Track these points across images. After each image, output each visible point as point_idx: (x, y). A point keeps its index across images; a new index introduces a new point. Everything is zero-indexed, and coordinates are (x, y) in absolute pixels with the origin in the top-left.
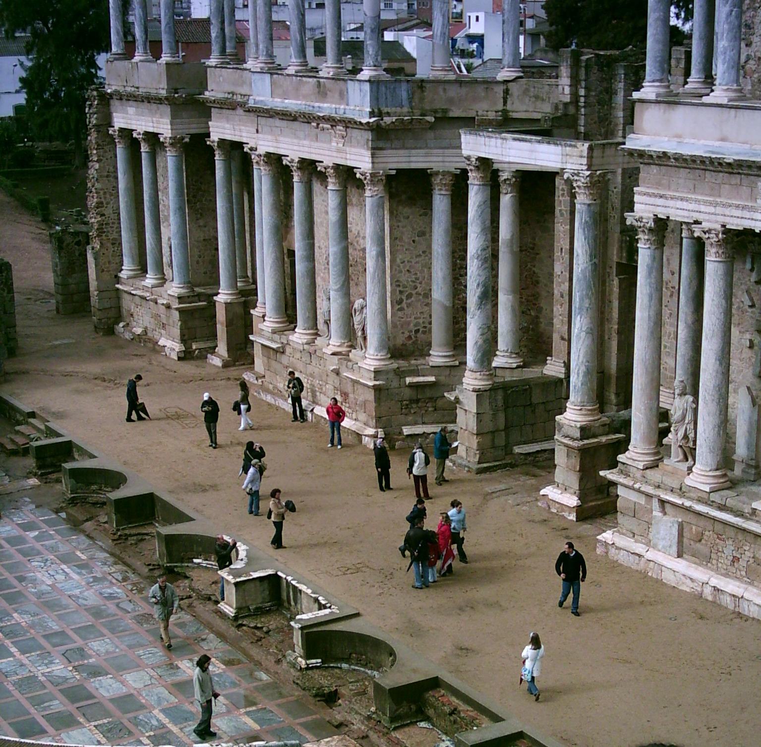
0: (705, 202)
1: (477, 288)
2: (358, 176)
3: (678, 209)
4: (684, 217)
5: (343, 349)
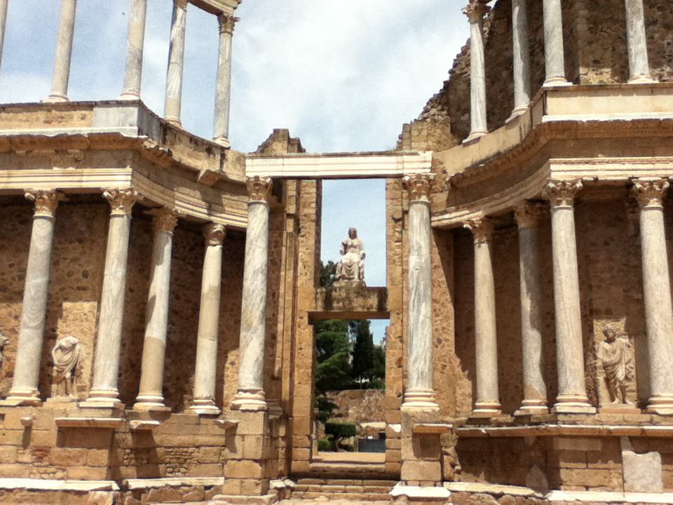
0: (642, 162)
1: (261, 302)
2: (106, 194)
3: (610, 169)
4: (617, 176)
5: (34, 398)
